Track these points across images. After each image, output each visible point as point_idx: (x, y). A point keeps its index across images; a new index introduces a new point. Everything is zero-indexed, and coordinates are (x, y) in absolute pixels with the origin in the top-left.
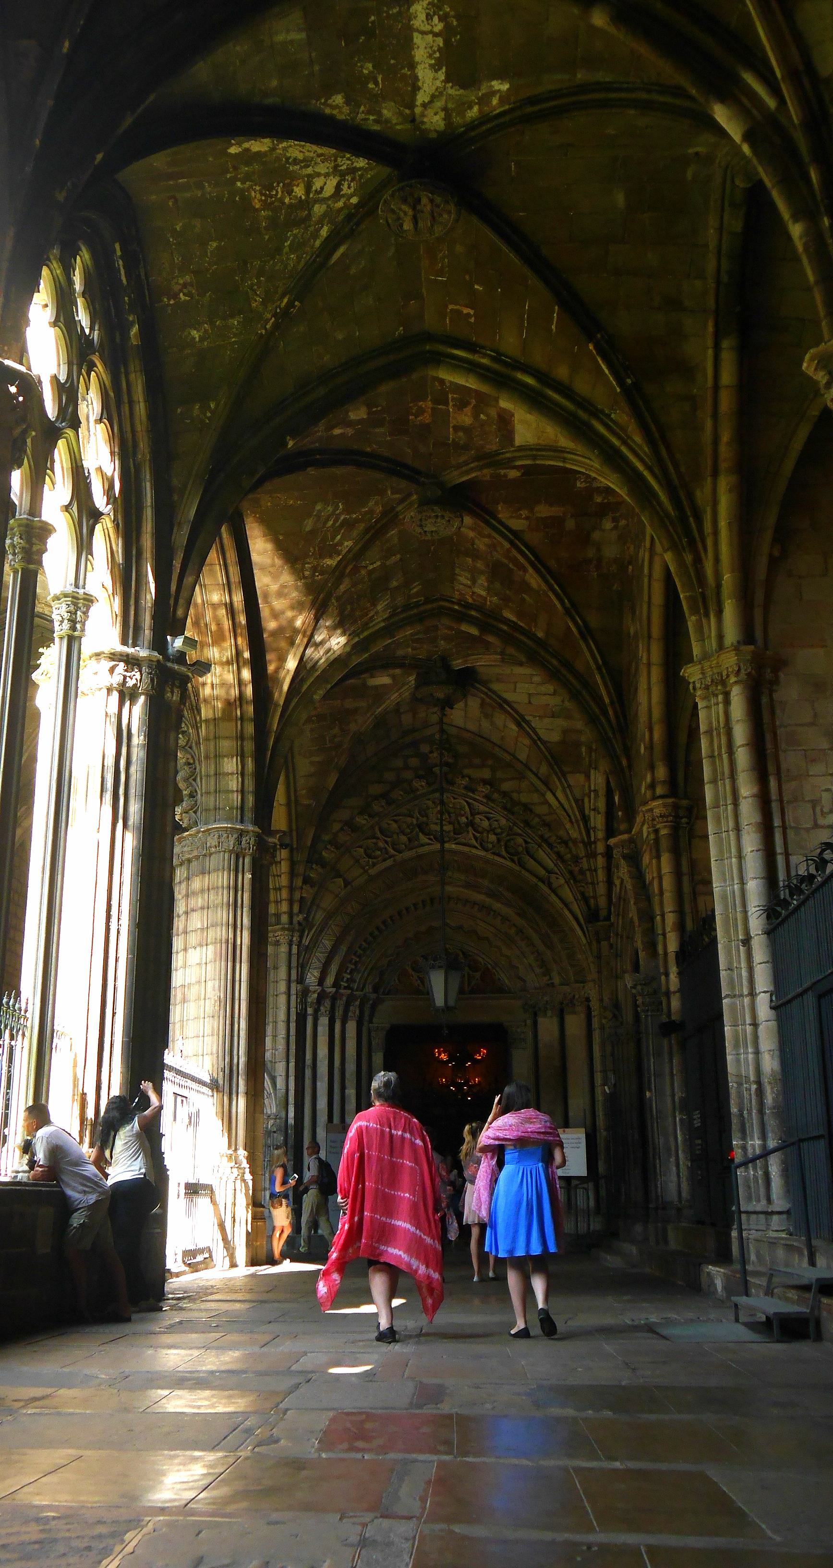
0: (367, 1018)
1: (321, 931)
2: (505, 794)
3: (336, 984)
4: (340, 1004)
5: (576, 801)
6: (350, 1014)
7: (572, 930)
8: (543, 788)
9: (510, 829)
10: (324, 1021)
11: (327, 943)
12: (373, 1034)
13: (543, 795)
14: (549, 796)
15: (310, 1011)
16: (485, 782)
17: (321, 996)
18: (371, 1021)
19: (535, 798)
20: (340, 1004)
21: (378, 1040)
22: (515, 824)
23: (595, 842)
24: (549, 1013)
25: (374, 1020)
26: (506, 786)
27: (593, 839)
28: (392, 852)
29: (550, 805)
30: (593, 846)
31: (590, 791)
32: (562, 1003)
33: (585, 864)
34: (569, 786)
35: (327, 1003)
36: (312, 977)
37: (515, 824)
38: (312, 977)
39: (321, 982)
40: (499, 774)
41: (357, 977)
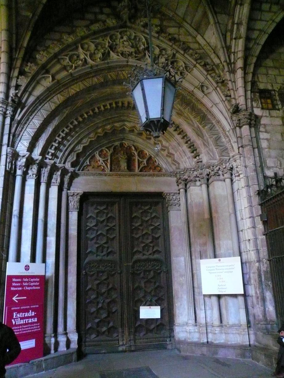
0: (66, 186)
1: (32, 112)
2: (170, 34)
3: (44, 153)
4: (45, 172)
5: (223, 35)
6: (53, 181)
7: (218, 122)
8: (194, 33)
9: (174, 55)
10: (31, 183)
11: (36, 122)
12: (70, 198)
13: (195, 38)
14: (199, 38)
15: (19, 172)
16: (156, 26)
17: (30, 162)
18: (69, 189)
19: (190, 39)
20: (45, 172)
21: (74, 203)
22: (177, 52)
23: (234, 63)
24: (198, 183)
25: (71, 188)
26: (172, 30)
27: (232, 61)
28: (89, 60)
29: (199, 44)
30: (233, 65)
31: (233, 23)
32: (208, 175)
33: (227, 76)
34: (218, 22)
35: (34, 170)
36: (22, 147)
37: (177, 52)
38: (22, 147)
39: (31, 148)
40: (165, 23)
41: (60, 154)
